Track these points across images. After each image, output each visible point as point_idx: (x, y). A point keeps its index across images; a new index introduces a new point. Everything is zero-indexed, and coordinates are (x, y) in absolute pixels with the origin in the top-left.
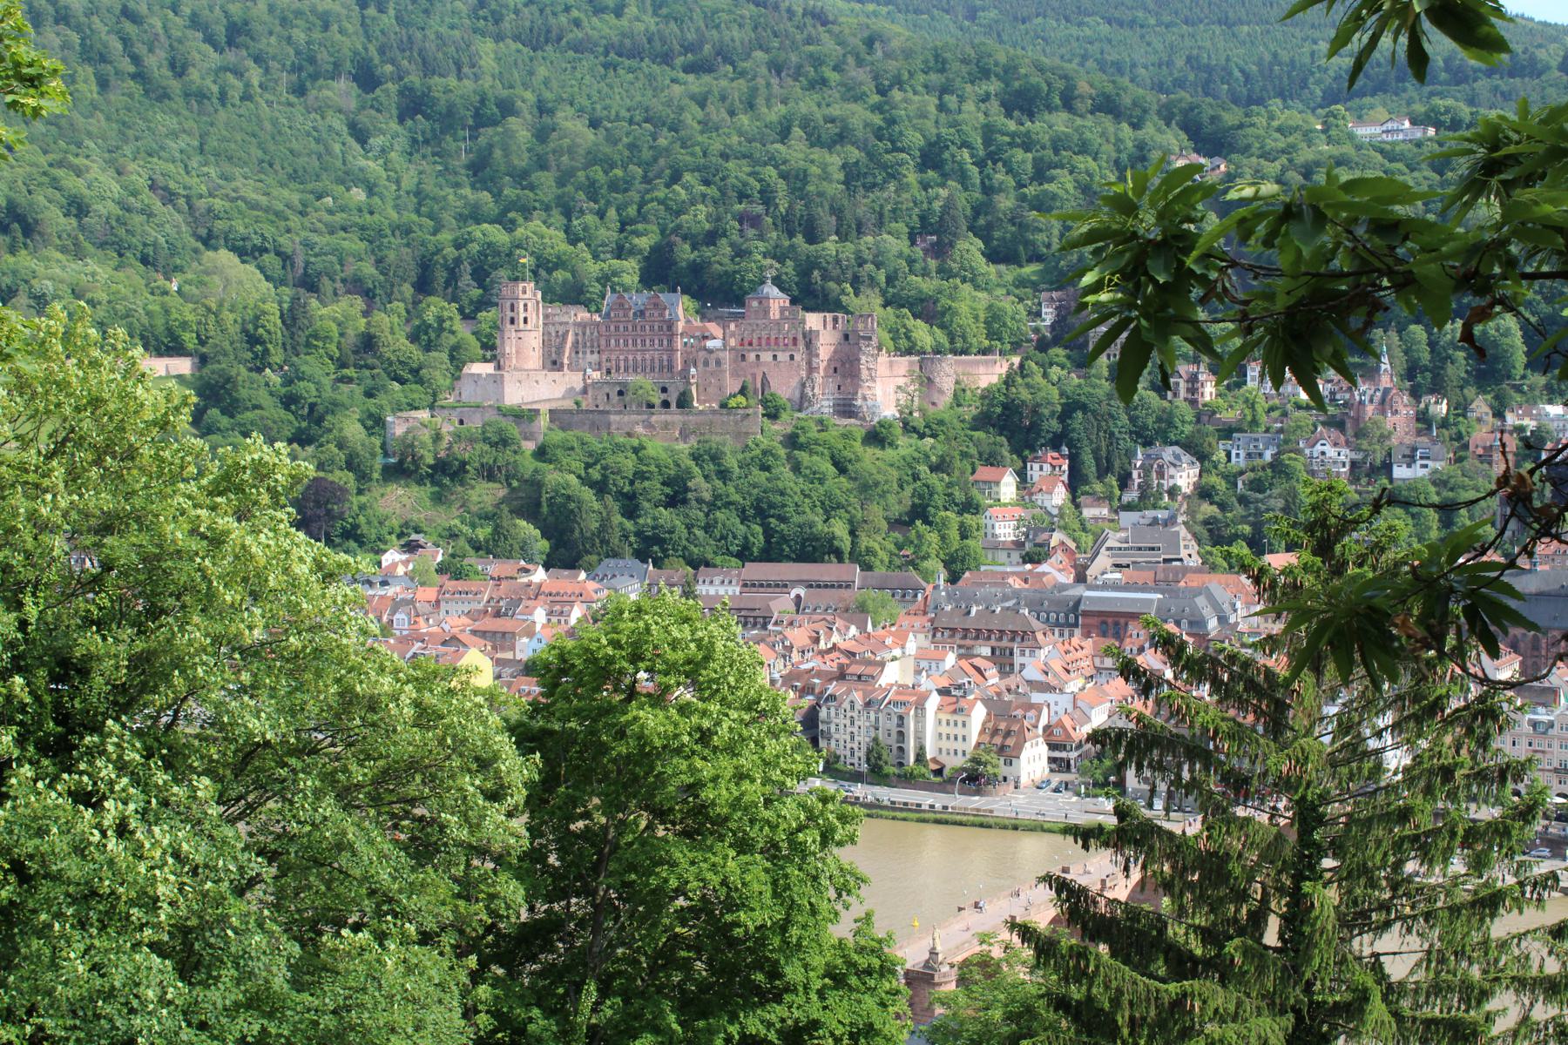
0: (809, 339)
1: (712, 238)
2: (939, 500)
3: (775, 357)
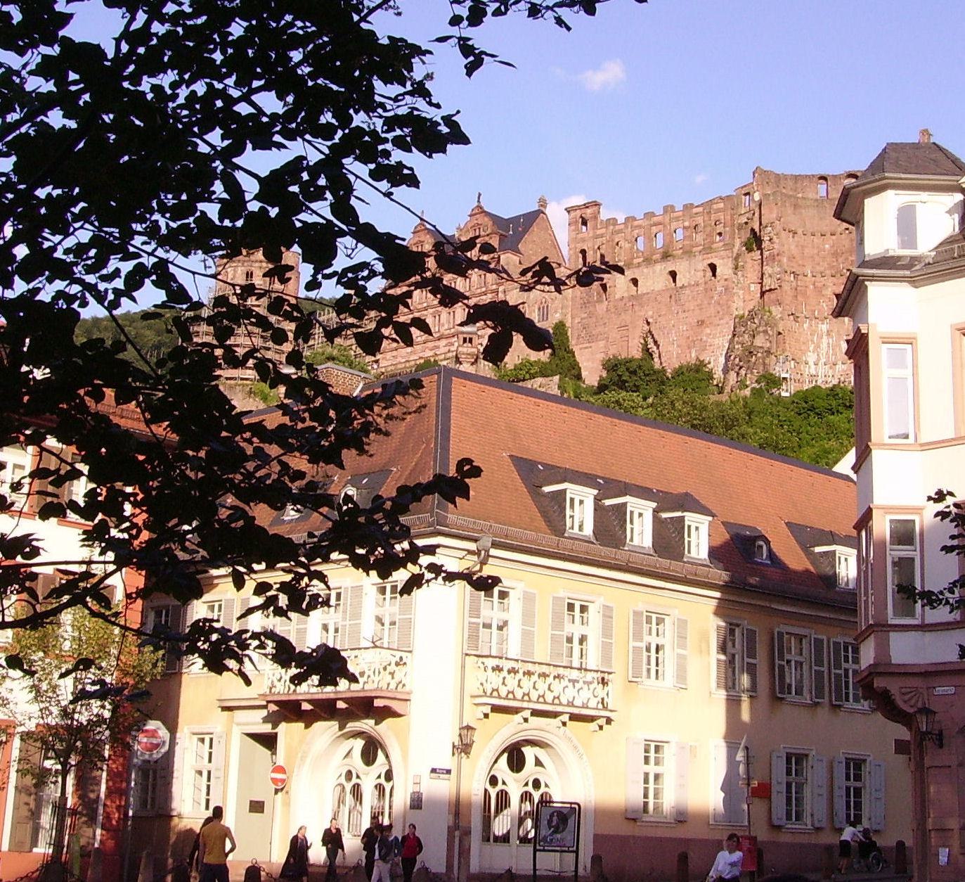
3: (673, 275)
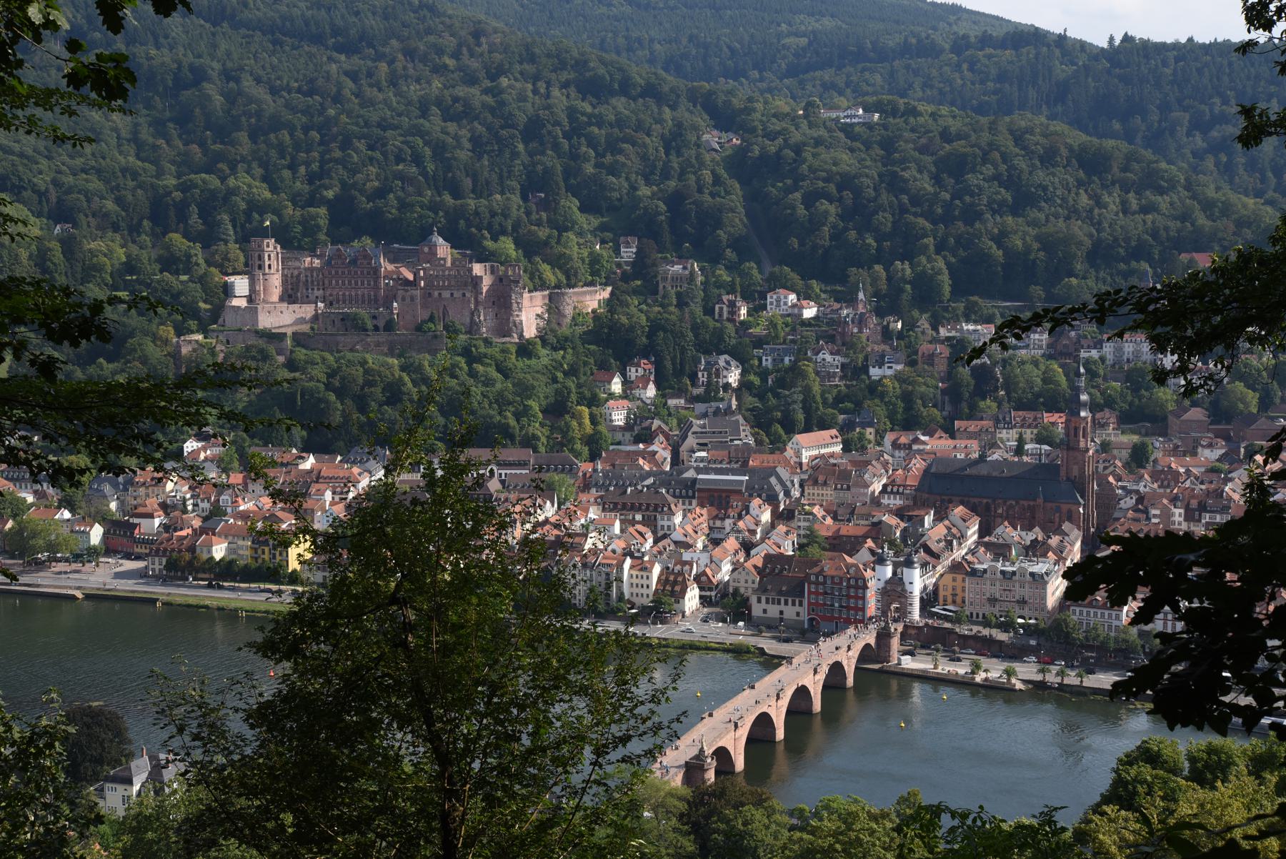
0: (477, 281)
1: (381, 193)
2: (574, 397)
